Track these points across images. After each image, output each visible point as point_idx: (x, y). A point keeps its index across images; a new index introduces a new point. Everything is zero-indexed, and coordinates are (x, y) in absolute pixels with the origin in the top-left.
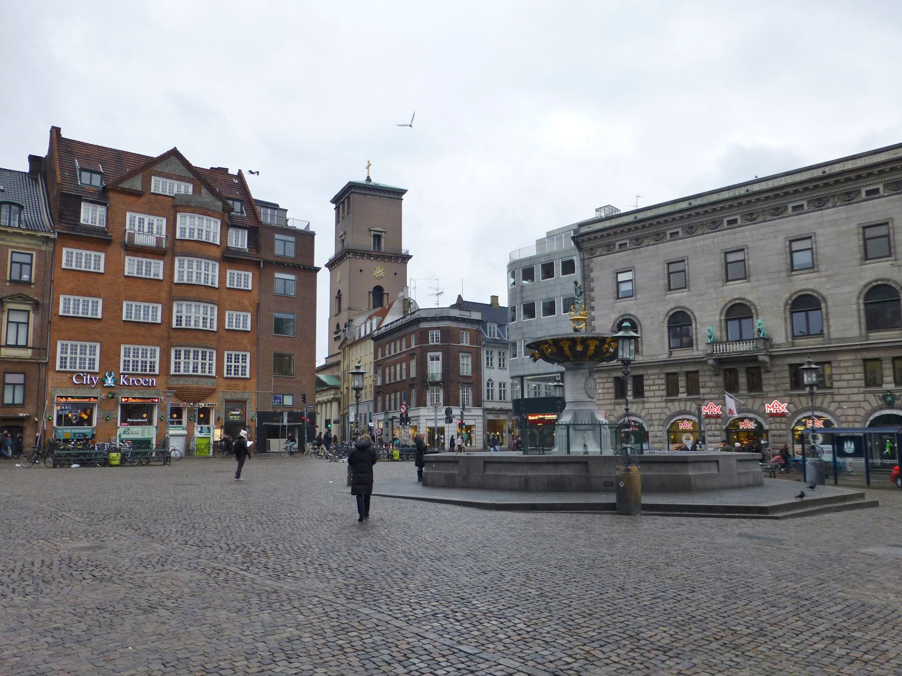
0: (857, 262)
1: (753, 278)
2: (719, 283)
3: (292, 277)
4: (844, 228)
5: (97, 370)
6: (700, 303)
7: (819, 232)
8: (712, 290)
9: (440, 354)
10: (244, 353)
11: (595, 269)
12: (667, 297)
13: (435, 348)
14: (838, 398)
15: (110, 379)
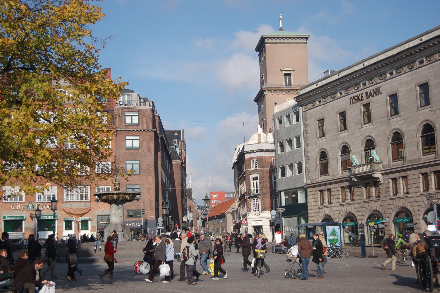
0: (416, 109)
1: (374, 122)
2: (360, 126)
3: (138, 138)
4: (410, 87)
5: (24, 201)
6: (352, 139)
7: (400, 89)
8: (357, 131)
9: (257, 175)
10: (108, 187)
11: (308, 118)
12: (339, 136)
13: (254, 172)
14: (411, 200)
15: (30, 206)
